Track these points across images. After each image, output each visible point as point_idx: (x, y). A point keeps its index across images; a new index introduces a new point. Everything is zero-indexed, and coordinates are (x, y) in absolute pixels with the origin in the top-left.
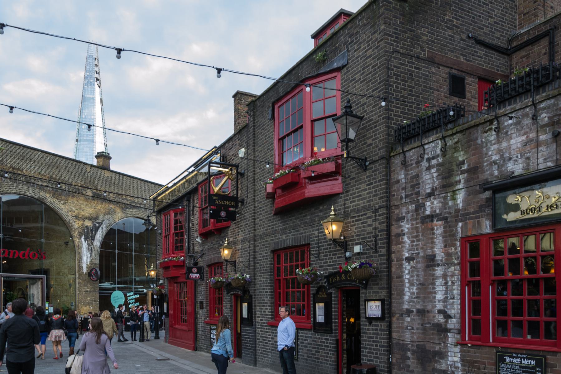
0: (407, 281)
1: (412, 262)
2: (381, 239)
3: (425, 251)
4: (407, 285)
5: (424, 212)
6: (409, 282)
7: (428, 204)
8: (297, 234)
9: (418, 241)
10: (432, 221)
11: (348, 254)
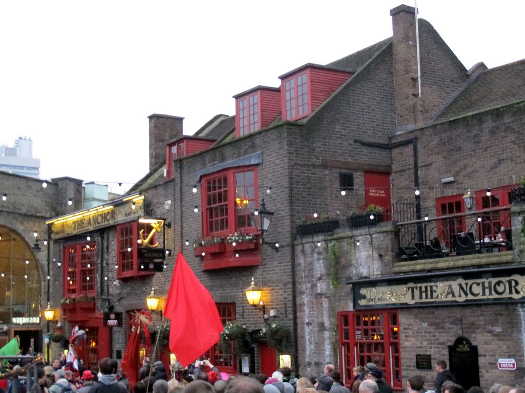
0: (307, 340)
1: (310, 326)
2: (289, 307)
3: (318, 318)
4: (308, 343)
5: (317, 290)
6: (309, 341)
7: (319, 285)
8: (224, 293)
9: (314, 311)
10: (322, 298)
11: (266, 316)
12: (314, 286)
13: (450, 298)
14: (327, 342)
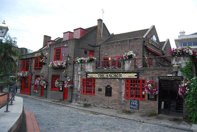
12: (78, 73)
13: (107, 77)
14: (79, 85)
